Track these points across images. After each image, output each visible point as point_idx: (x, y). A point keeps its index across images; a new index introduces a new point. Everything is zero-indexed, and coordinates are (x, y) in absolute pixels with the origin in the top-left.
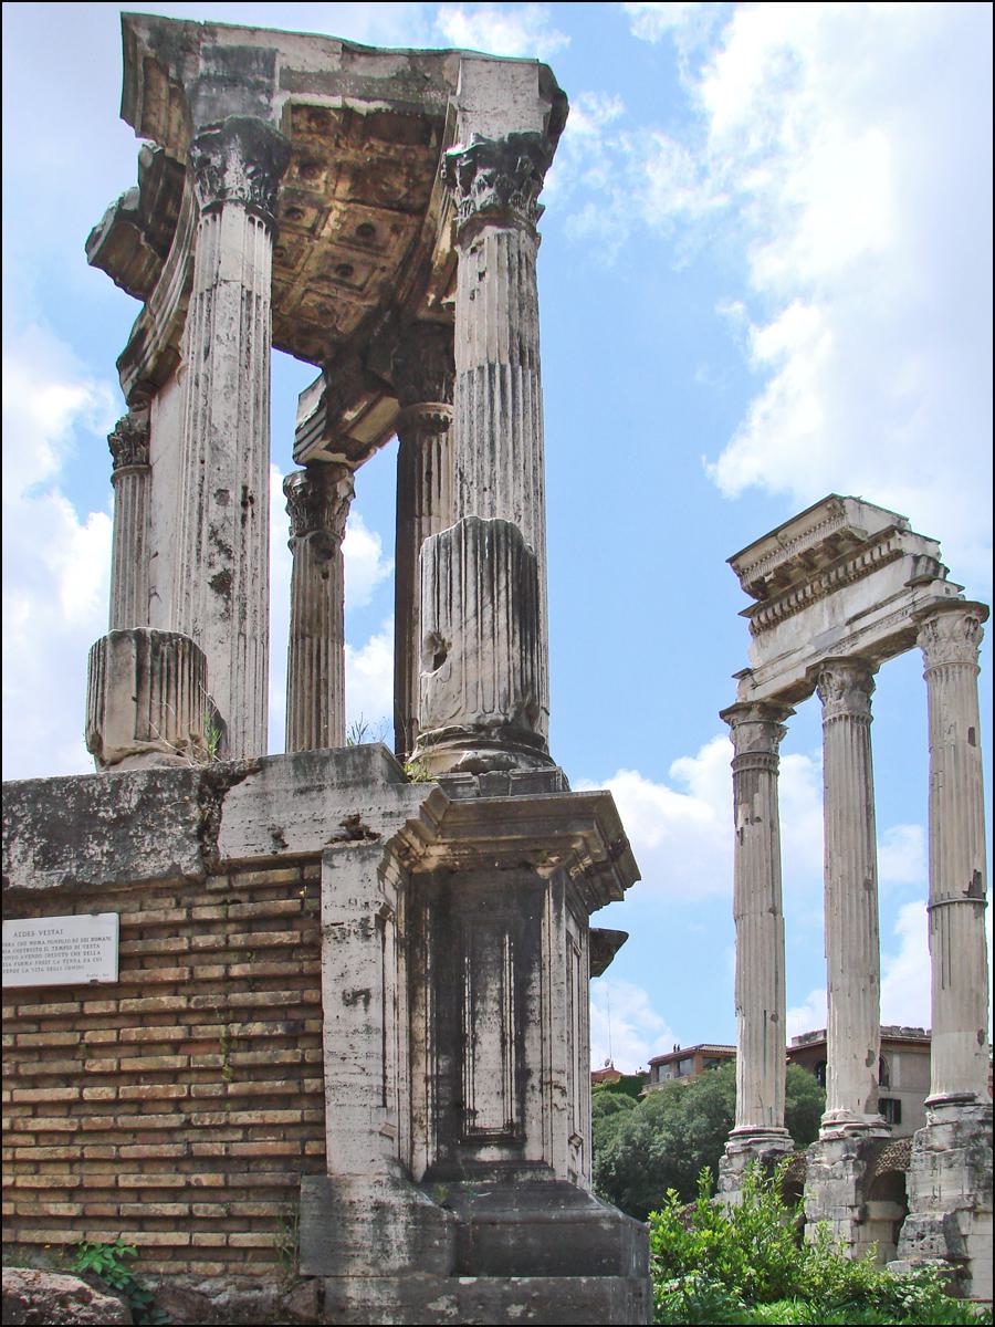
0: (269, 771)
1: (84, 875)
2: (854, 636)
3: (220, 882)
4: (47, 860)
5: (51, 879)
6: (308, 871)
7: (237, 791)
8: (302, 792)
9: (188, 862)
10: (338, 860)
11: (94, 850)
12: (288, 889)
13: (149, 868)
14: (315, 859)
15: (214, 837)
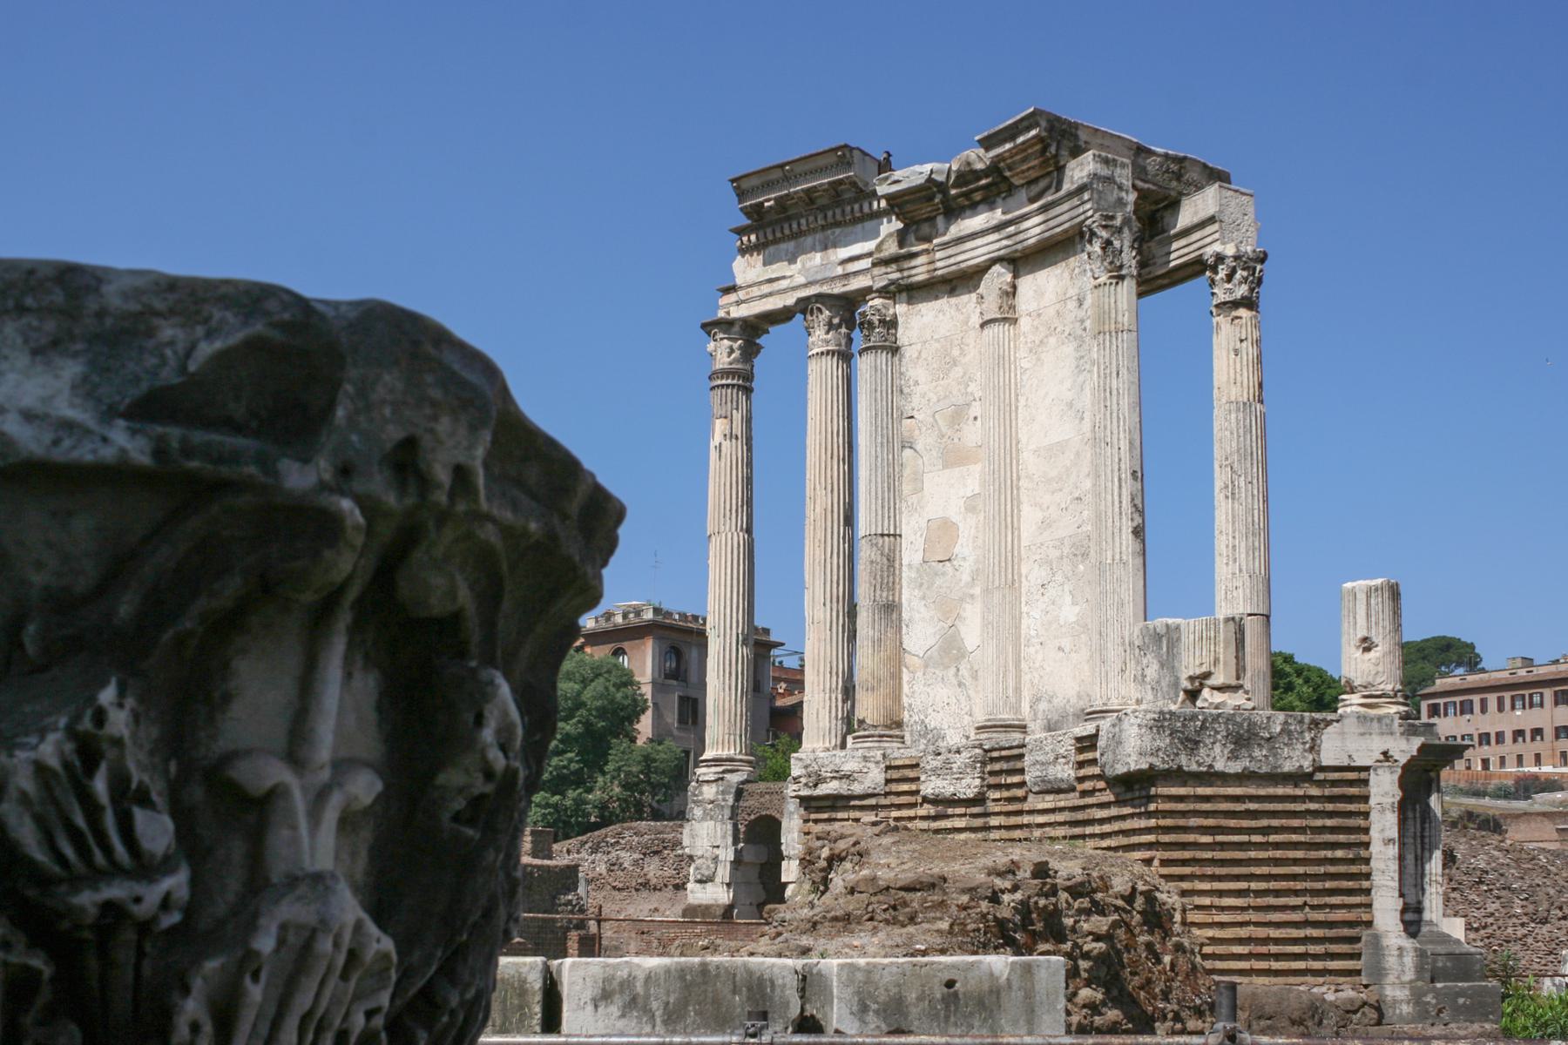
0: (1346, 721)
1: (1253, 767)
2: (846, 276)
3: (1320, 776)
4: (1233, 756)
5: (1235, 767)
6: (1363, 775)
7: (1330, 729)
8: (1362, 734)
9: (1307, 765)
10: (1380, 771)
11: (1257, 753)
12: (1351, 783)
13: (1288, 767)
14: (1367, 769)
15: (1318, 753)
